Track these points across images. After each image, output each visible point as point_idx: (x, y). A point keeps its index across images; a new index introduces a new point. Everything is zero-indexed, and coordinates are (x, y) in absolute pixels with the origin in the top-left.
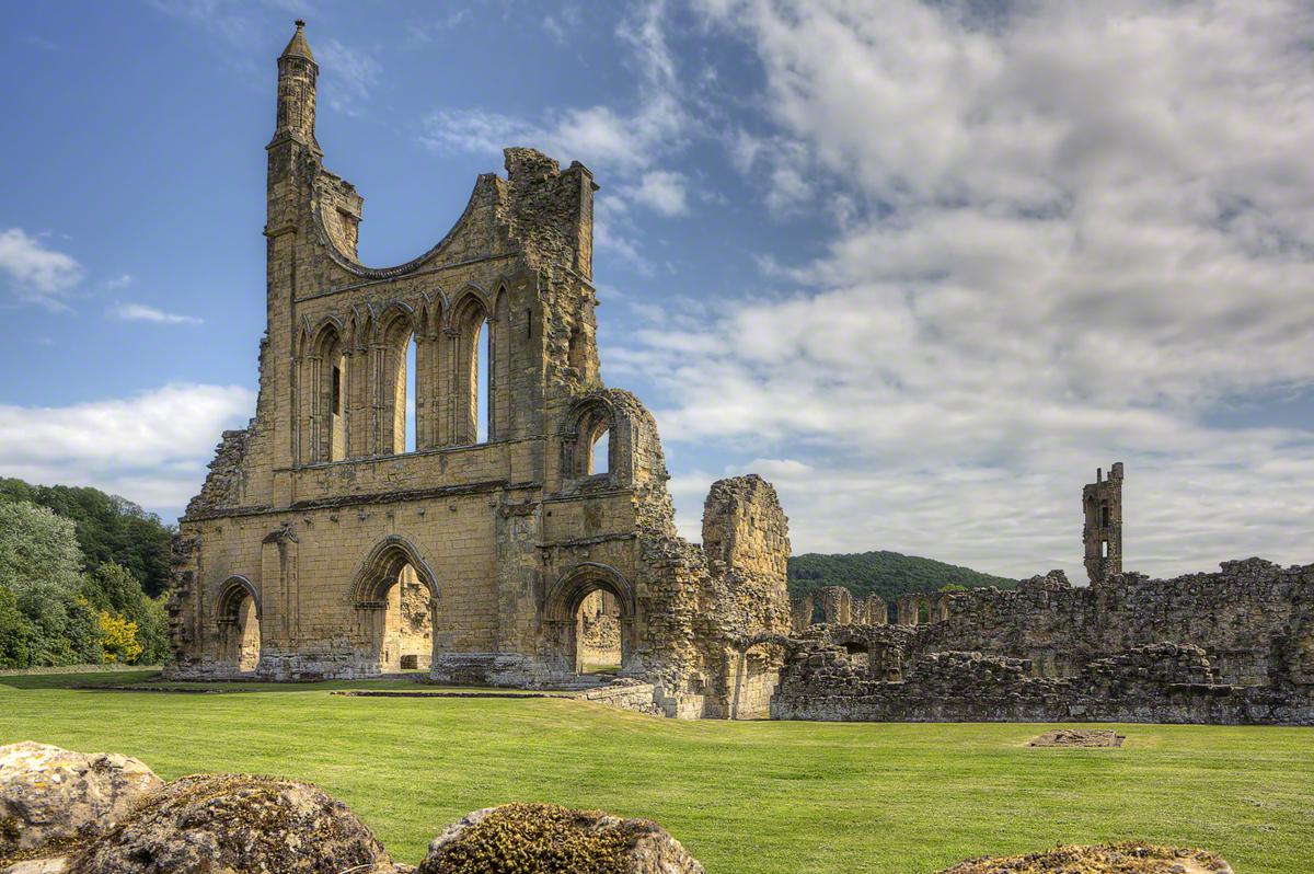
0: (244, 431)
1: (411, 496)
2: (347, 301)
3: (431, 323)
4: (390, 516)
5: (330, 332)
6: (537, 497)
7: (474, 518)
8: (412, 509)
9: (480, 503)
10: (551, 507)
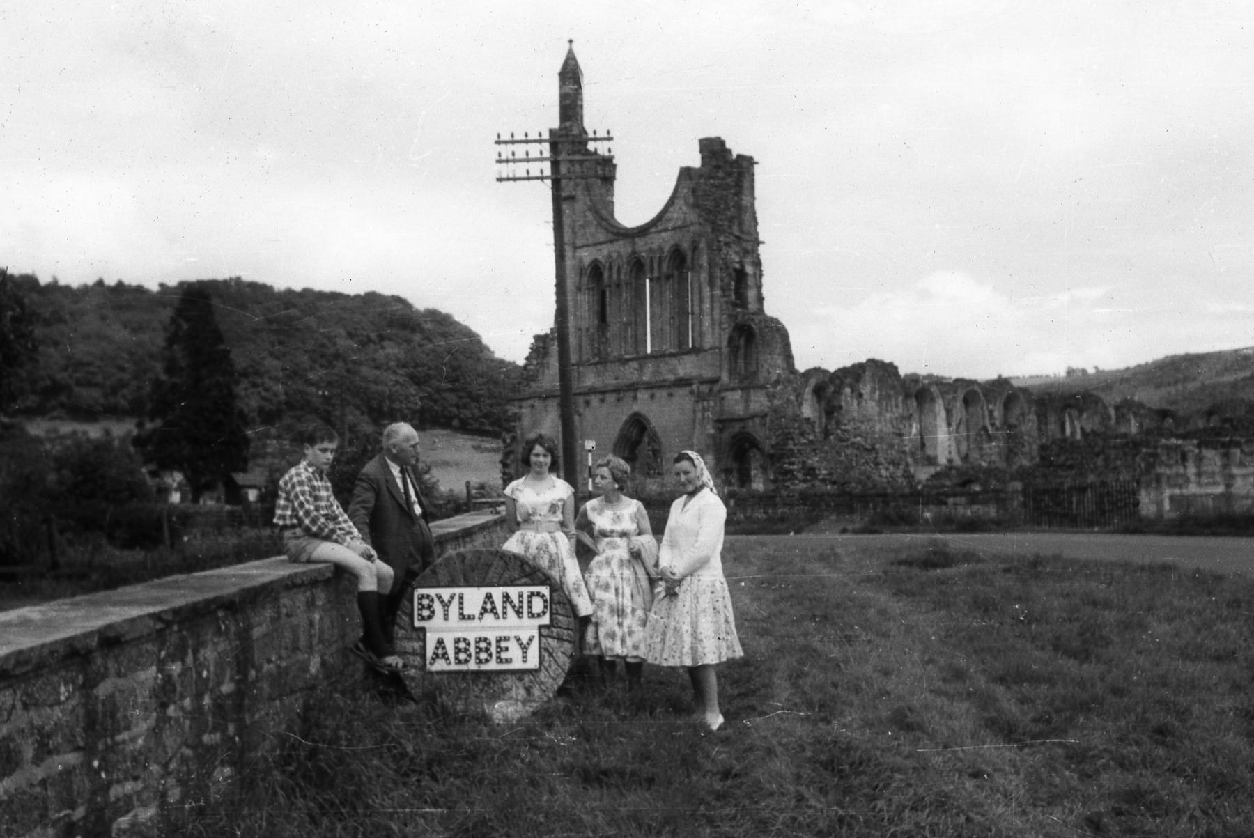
0: (546, 336)
1: (649, 386)
2: (605, 250)
3: (656, 267)
4: (635, 398)
5: (596, 270)
6: (716, 388)
7: (683, 398)
8: (649, 392)
9: (686, 390)
10: (723, 394)
